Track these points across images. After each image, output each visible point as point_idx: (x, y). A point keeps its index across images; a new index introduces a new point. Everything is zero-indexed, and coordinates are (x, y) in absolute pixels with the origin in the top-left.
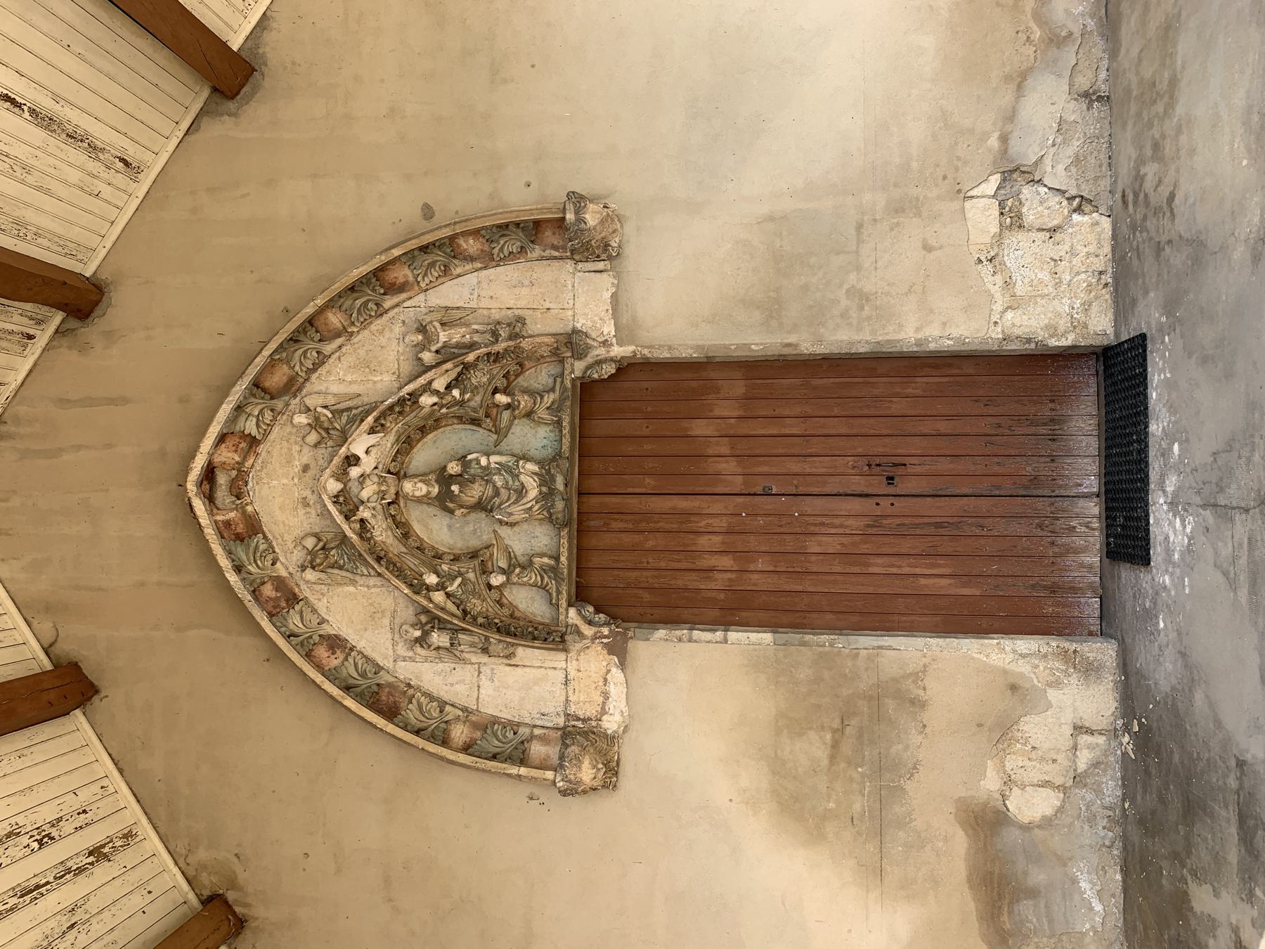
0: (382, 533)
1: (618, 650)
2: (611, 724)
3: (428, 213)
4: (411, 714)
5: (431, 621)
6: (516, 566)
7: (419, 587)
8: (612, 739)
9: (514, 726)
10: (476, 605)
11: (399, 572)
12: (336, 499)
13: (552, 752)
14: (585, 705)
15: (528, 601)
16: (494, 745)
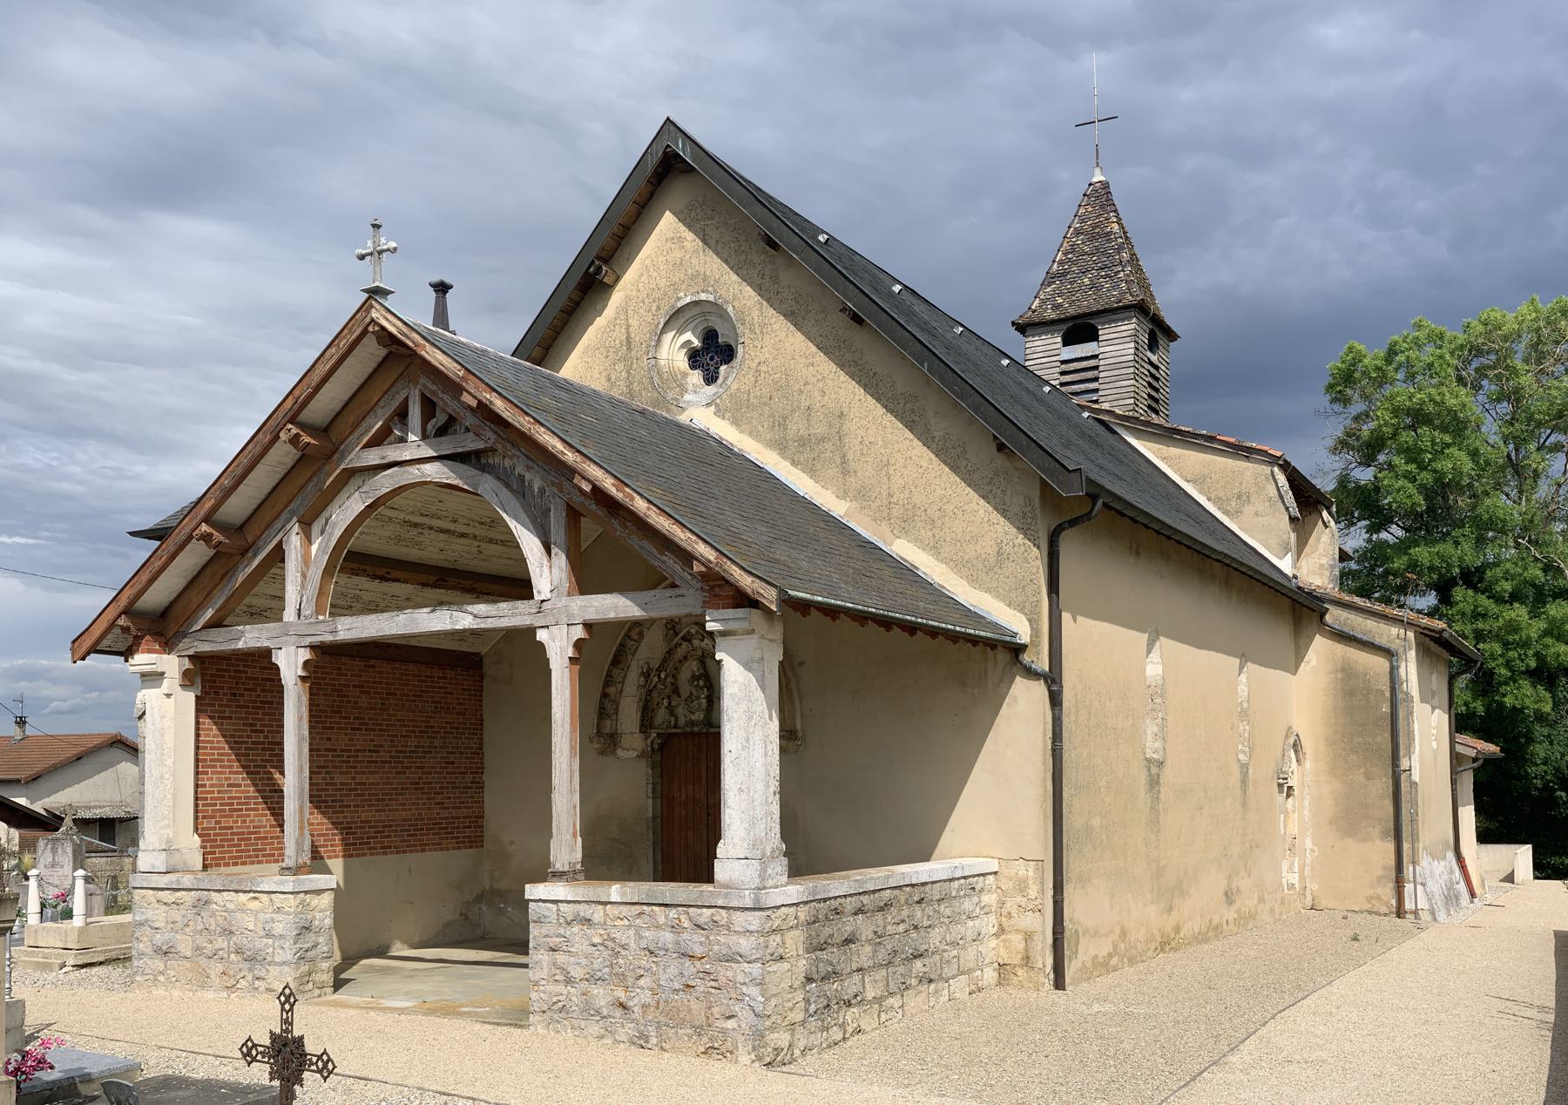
0: (680, 652)
1: (642, 755)
2: (619, 752)
3: (801, 664)
4: (615, 672)
5: (647, 675)
6: (671, 711)
7: (659, 670)
8: (614, 752)
9: (617, 712)
10: (655, 695)
11: (665, 661)
12: (1067, 342)
13: (608, 730)
14: (626, 741)
15: (661, 716)
16: (608, 704)
